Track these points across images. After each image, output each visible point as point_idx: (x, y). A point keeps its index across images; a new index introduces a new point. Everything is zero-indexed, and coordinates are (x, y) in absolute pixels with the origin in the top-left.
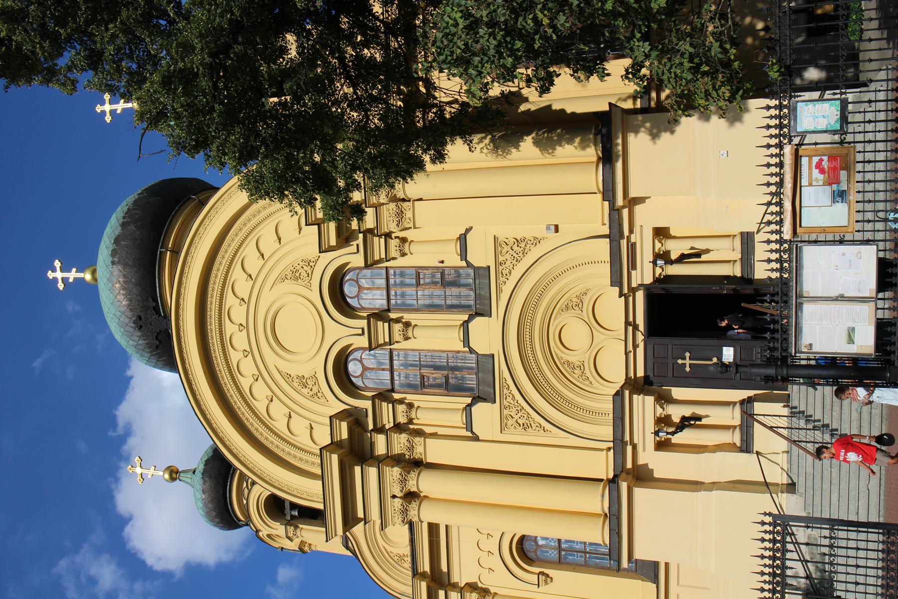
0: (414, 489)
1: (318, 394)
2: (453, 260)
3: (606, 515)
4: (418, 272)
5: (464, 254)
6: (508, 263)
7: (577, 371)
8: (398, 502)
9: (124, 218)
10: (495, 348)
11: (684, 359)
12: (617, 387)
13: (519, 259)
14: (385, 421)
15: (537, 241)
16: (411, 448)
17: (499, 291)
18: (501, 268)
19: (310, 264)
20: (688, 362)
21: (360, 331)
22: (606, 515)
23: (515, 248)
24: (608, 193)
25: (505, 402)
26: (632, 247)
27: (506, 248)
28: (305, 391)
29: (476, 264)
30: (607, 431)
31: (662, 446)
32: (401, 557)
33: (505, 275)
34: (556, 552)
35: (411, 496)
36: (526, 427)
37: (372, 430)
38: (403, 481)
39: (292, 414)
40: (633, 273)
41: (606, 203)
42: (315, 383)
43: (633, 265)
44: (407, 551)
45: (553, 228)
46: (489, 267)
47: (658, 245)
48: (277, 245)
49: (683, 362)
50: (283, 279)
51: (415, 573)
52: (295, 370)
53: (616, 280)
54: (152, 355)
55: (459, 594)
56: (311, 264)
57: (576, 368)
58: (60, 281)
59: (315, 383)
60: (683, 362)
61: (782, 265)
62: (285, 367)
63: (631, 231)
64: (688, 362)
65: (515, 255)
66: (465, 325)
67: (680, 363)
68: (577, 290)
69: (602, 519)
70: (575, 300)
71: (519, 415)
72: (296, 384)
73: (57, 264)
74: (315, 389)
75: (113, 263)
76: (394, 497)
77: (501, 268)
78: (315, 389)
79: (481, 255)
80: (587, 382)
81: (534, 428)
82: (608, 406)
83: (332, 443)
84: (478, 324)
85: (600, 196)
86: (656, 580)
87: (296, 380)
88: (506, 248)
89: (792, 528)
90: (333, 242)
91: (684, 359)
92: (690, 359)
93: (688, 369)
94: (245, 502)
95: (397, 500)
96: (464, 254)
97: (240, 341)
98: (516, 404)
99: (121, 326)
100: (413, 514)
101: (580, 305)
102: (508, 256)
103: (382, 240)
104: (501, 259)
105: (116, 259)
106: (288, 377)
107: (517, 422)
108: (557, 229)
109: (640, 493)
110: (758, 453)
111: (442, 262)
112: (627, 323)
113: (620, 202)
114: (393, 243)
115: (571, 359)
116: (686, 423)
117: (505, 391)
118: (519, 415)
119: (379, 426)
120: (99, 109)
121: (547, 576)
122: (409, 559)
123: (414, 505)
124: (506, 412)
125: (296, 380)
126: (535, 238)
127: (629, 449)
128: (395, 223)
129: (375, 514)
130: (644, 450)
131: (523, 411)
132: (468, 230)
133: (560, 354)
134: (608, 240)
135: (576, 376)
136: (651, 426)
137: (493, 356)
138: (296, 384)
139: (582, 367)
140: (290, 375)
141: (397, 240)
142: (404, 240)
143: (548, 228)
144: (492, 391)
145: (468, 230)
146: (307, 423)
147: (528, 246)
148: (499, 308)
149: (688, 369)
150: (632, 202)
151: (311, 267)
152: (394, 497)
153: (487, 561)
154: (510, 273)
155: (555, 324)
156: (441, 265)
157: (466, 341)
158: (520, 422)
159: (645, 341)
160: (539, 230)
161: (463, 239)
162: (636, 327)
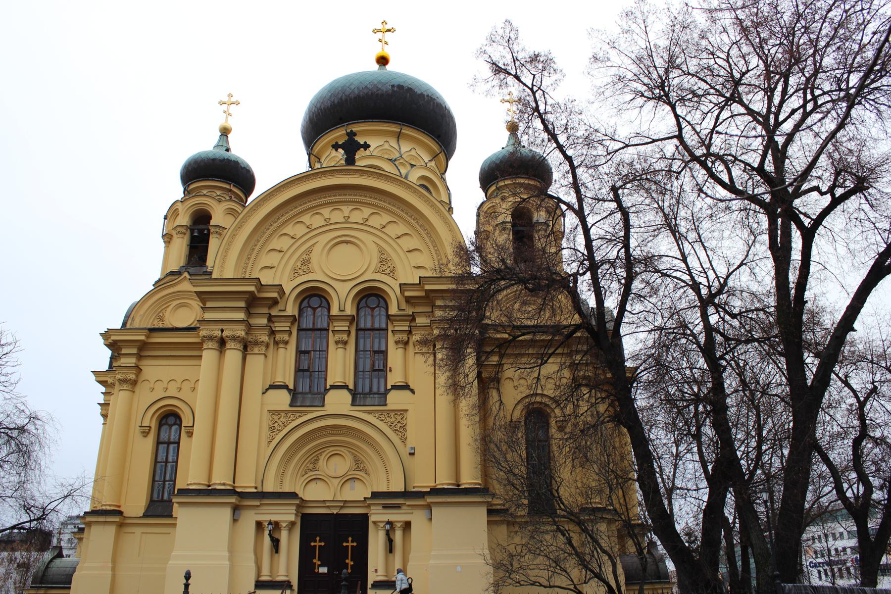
0: (228, 346)
1: (296, 274)
2: (394, 378)
3: (209, 486)
4: (384, 353)
5: (395, 387)
6: (388, 419)
7: (311, 466)
8: (218, 333)
9: (428, 96)
12: (301, 495)
14: (276, 324)
15: (404, 440)
16: (256, 343)
17: (370, 412)
18: (385, 414)
19: (392, 273)
21: (342, 308)
22: (209, 486)
23: (399, 425)
24: (435, 492)
26: (398, 507)
27: (399, 418)
28: (299, 264)
29: (388, 396)
30: (269, 487)
31: (259, 524)
32: (161, 319)
34: (166, 440)
35: (222, 343)
36: (272, 428)
37: (270, 314)
38: (234, 338)
39: (283, 253)
40: (381, 507)
41: (428, 490)
43: (385, 507)
44: (167, 325)
45: (413, 451)
46: (386, 405)
47: (399, 525)
48: (406, 250)
50: (382, 251)
51: (152, 330)
52: (315, 257)
53: (376, 495)
54: (318, 110)
55: (133, 365)
62: (317, 250)
63: (409, 506)
66: (345, 387)
68: (368, 467)
70: (362, 465)
72: (305, 256)
74: (300, 272)
75: (393, 86)
76: (222, 331)
77: (385, 414)
78: (300, 272)
79: (395, 399)
80: (304, 473)
82: (286, 489)
83: (262, 285)
84: (346, 396)
85: (433, 484)
86: (145, 516)
87: (307, 257)
88: (399, 418)
90: (407, 294)
92: (320, 546)
94: (205, 192)
95: (220, 332)
96: (395, 387)
97: (337, 217)
99: (342, 88)
100: (210, 344)
101: (358, 469)
102: (393, 419)
103: (407, 328)
104: (392, 414)
105: (396, 89)
106: (309, 251)
108: (412, 454)
109: (227, 512)
111: (390, 371)
112: (346, 501)
113: (429, 500)
114: (405, 337)
115: (321, 462)
116: (276, 544)
117: (298, 414)
119: (273, 319)
121: (148, 433)
122: (161, 326)
124: (283, 414)
125: (307, 257)
126: (406, 438)
127: (258, 503)
128: (419, 339)
129: (209, 316)
130: (256, 514)
132: (413, 391)
133: (324, 454)
134: (403, 490)
135: (308, 465)
136: (274, 518)
137: (323, 406)
138: (304, 257)
139: (315, 469)
141: (406, 339)
142: (406, 343)
143: (413, 448)
144: (298, 404)
145: (413, 391)
146: (275, 264)
148: (357, 412)
149: (313, 544)
150: (429, 507)
152: (222, 331)
153: (159, 387)
154: (382, 420)
155: (345, 451)
156: (388, 369)
157: (333, 387)
158: (276, 425)
159: (333, 514)
160: (410, 443)
161: (406, 387)
162: (342, 507)
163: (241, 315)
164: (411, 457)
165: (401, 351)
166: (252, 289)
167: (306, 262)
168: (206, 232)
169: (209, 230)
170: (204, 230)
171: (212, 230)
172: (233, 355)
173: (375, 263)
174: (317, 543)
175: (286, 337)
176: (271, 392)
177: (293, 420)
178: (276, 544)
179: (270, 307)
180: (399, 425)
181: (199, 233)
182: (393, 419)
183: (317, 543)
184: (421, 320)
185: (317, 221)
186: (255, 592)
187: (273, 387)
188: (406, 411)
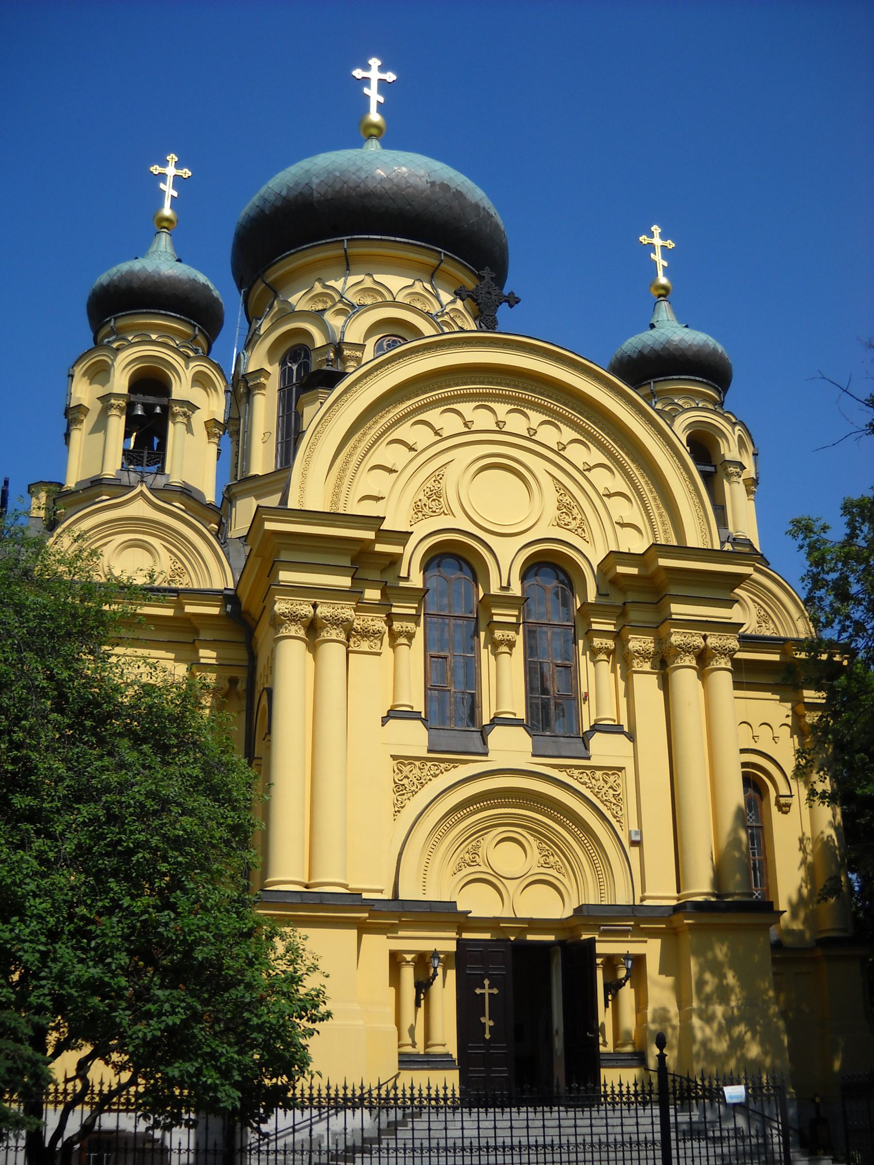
0: (324, 635)
1: (420, 514)
5: (596, 728)
6: (593, 781)
10: (497, 759)
11: (483, 987)
13: (600, 796)
19: (581, 529)
20: (486, 991)
25: (429, 764)
33: (580, 776)
36: (399, 788)
38: (336, 622)
42: (435, 512)
45: (638, 838)
46: (589, 758)
49: (487, 986)
52: (449, 486)
56: (580, 530)
57: (474, 856)
58: (366, 74)
59: (435, 512)
60: (487, 986)
61: (433, 1099)
64: (486, 991)
65: (603, 791)
67: (485, 982)
69: (306, 881)
71: (416, 782)
73: (390, 77)
75: (433, 184)
76: (315, 606)
81: (399, 798)
89: (313, 1115)
91: (483, 987)
93: (478, 991)
97: (482, 419)
98: (428, 778)
104: (598, 774)
106: (438, 476)
107: (405, 777)
110: (398, 1075)
116: (423, 986)
118: (416, 782)
120: (656, 229)
123: (302, 633)
131: (419, 787)
137: (486, 754)
140: (441, 479)
147: (614, 807)
151: (576, 530)
152: (315, 606)
161: (615, 729)
163: (345, 582)
164: (636, 850)
165: (605, 667)
166: (370, 535)
167: (435, 495)
168: (158, 410)
169: (166, 409)
170: (153, 406)
171: (176, 409)
172: (333, 653)
173: (552, 511)
174: (486, 990)
175: (411, 626)
176: (392, 722)
177: (436, 776)
178: (423, 986)
179: (383, 571)
180: (611, 792)
181: (144, 410)
182: (601, 783)
183: (486, 990)
184: (634, 615)
185: (449, 423)
186: (398, 1075)
187: (393, 714)
188: (621, 769)
